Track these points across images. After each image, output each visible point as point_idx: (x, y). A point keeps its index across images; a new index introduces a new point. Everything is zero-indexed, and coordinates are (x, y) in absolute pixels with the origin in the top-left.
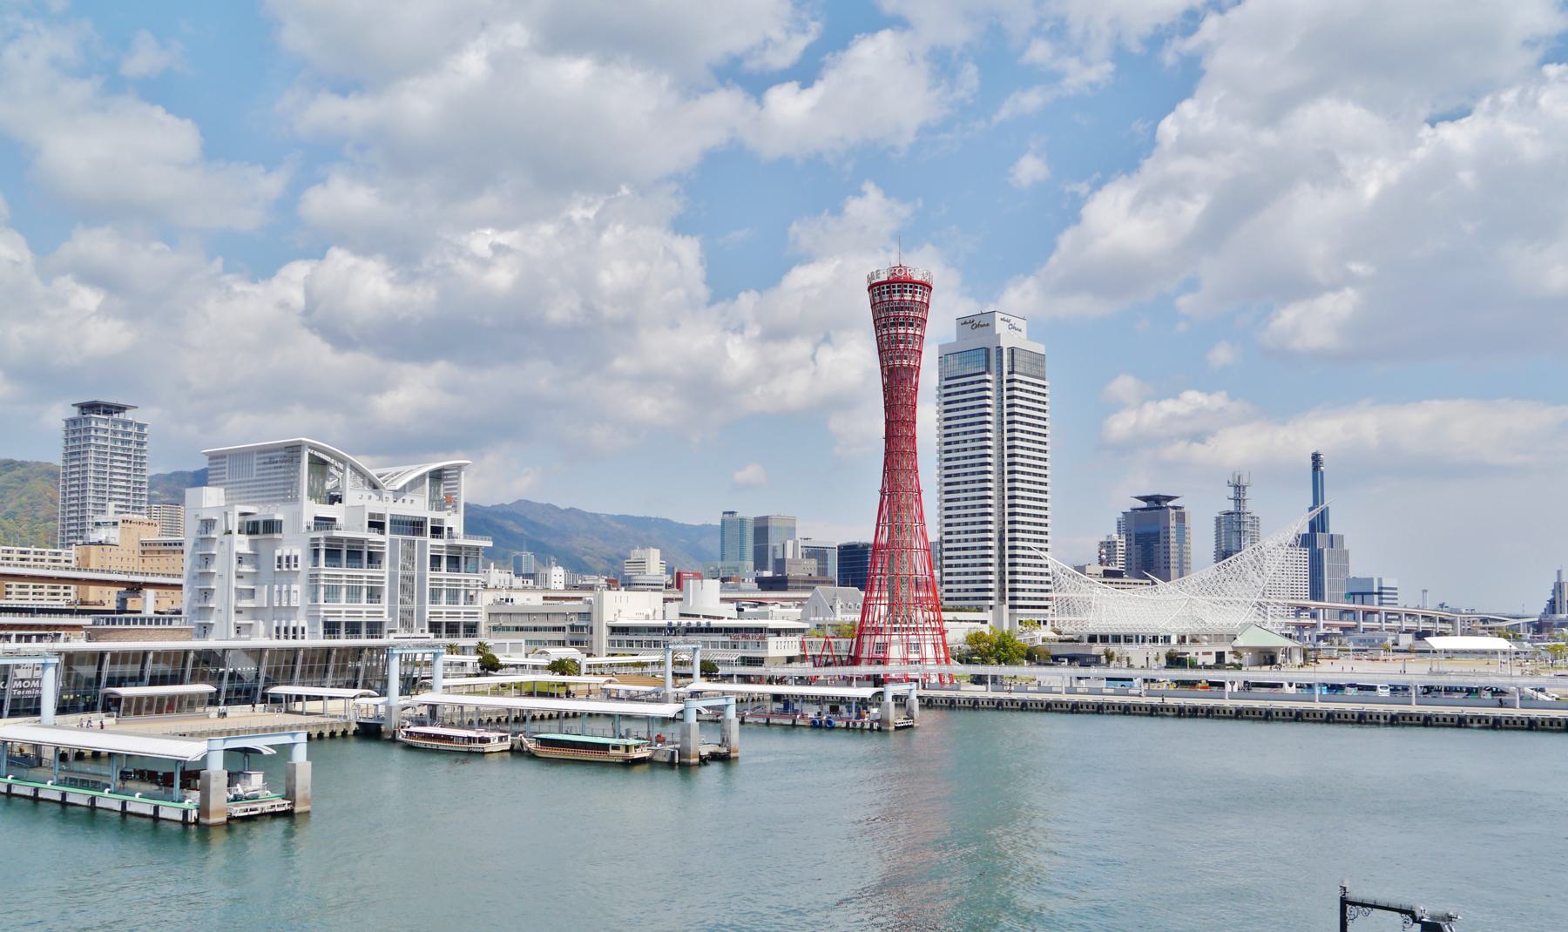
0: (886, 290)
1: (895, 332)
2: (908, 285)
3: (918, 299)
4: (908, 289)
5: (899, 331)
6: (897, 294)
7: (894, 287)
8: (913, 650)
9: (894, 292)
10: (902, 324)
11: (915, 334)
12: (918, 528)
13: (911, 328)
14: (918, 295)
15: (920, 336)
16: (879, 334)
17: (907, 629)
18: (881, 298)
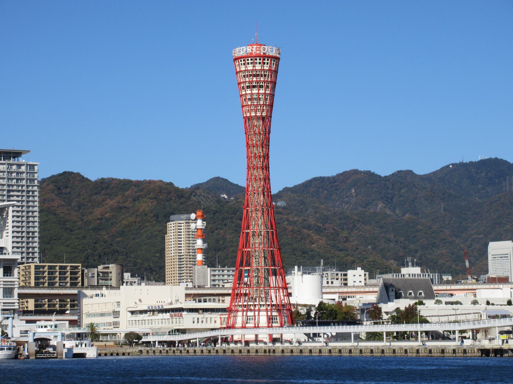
0: (243, 62)
1: (250, 92)
4: (258, 61)
5: (253, 92)
7: (248, 60)
9: (248, 63)
10: (254, 87)
11: (265, 93)
14: (266, 65)
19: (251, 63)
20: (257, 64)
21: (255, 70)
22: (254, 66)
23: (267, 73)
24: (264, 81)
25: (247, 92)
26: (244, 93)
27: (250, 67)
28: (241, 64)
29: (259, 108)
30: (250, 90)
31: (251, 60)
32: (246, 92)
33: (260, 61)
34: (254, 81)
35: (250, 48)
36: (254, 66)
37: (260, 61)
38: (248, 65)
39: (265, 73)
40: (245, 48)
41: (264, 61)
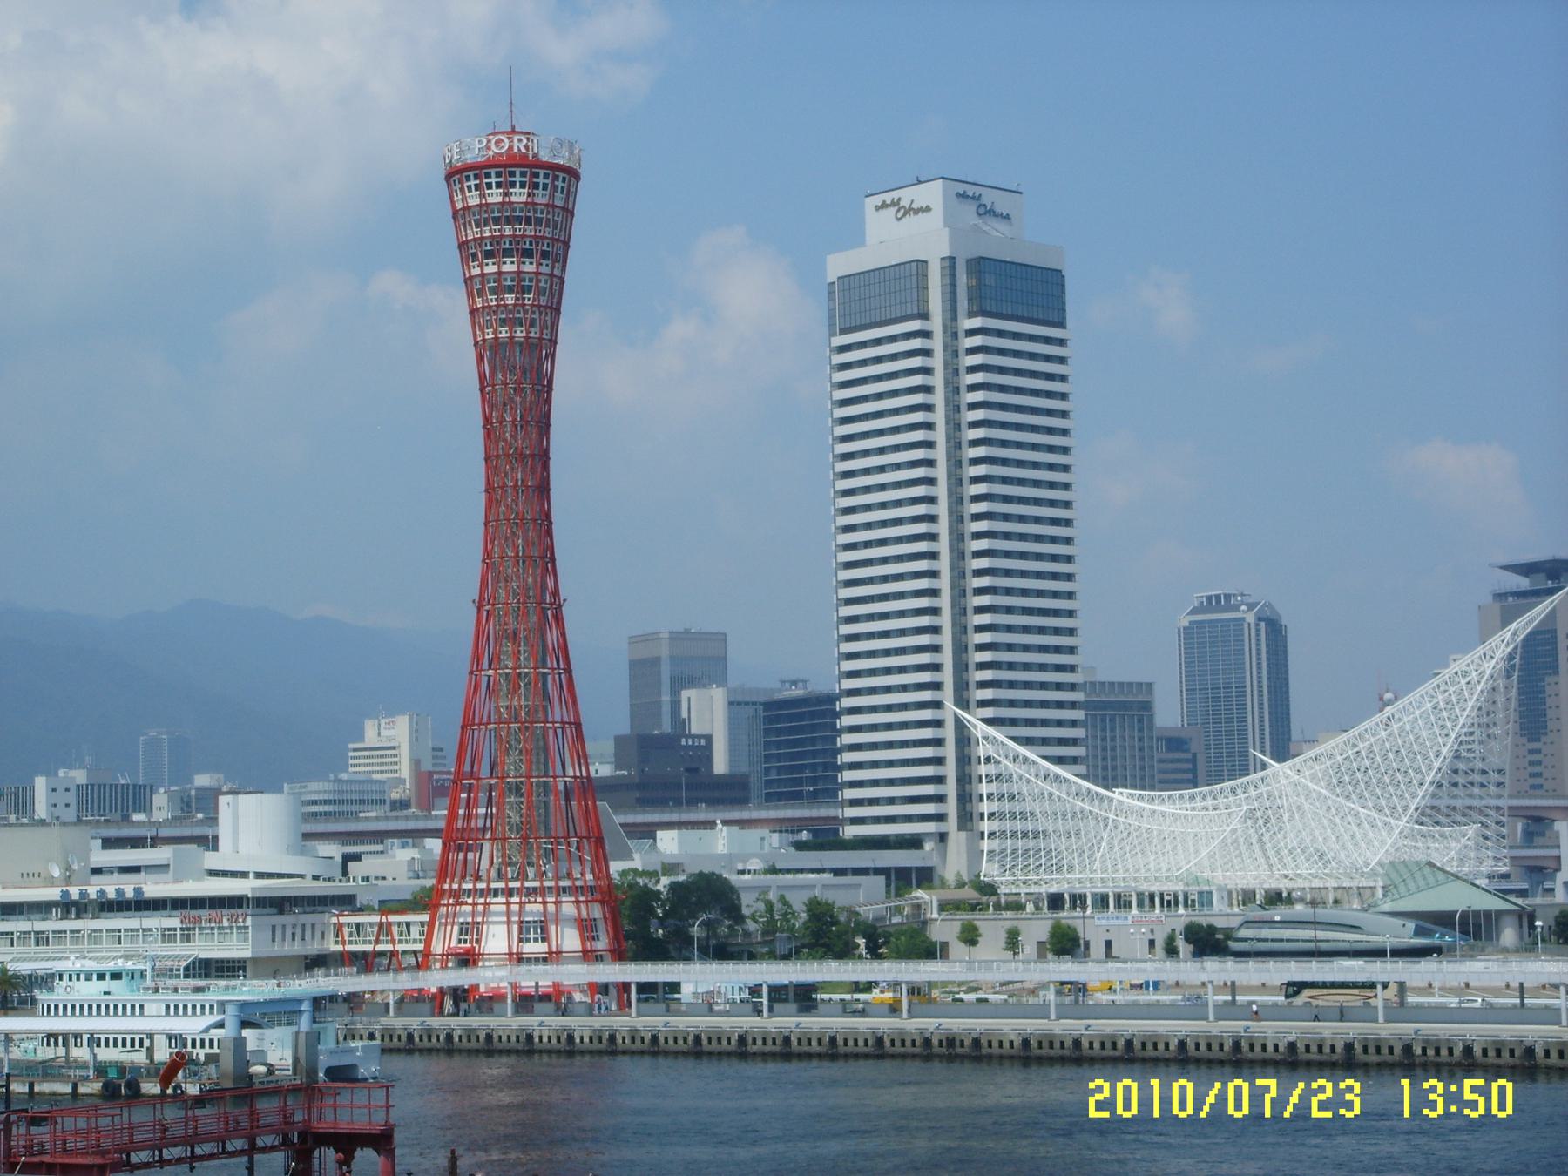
2: (518, 171)
3: (541, 198)
5: (505, 268)
6: (494, 190)
8: (532, 936)
12: (563, 676)
13: (544, 262)
14: (540, 191)
15: (552, 275)
16: (477, 271)
17: (519, 890)
18: (483, 196)
19: (499, 185)
20: (538, 188)
21: (510, 203)
22: (506, 194)
23: (560, 218)
24: (535, 237)
25: (488, 270)
26: (491, 268)
27: (495, 196)
28: (469, 187)
29: (521, 316)
30: (494, 264)
31: (523, 174)
32: (482, 270)
33: (546, 181)
34: (486, 238)
35: (520, 140)
36: (506, 194)
37: (546, 181)
38: (511, 190)
39: (539, 215)
40: (506, 140)
41: (535, 180)
